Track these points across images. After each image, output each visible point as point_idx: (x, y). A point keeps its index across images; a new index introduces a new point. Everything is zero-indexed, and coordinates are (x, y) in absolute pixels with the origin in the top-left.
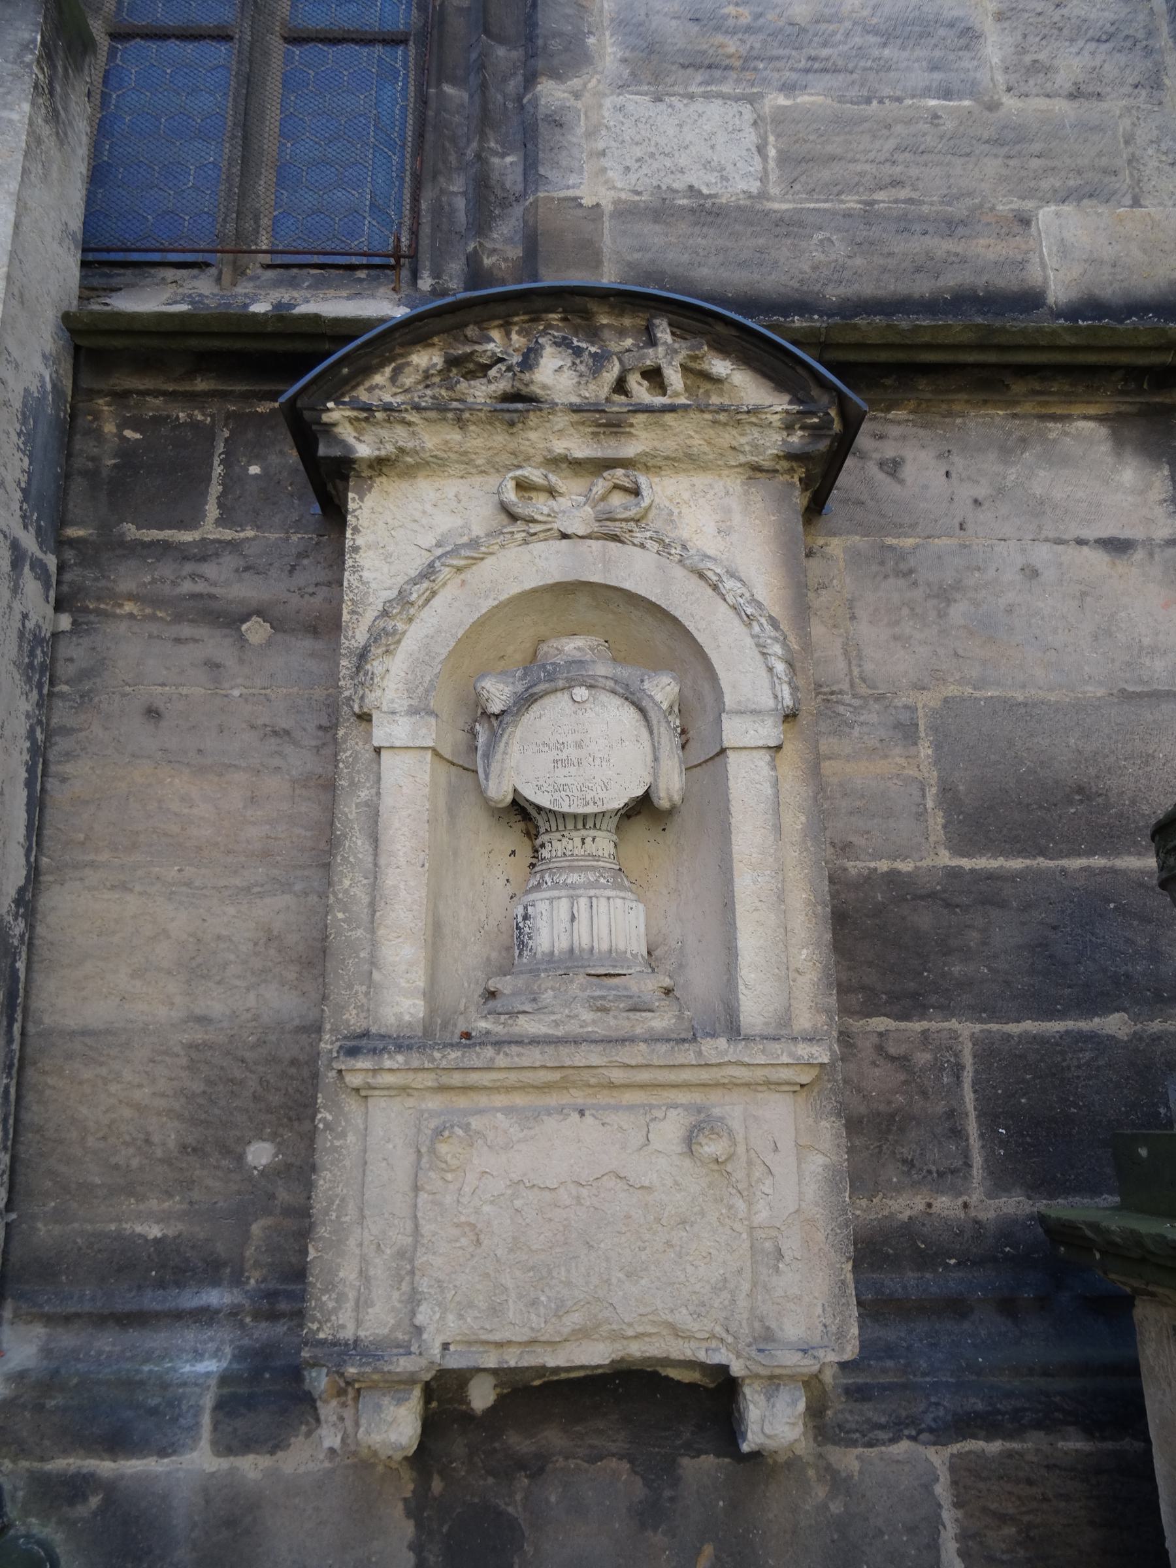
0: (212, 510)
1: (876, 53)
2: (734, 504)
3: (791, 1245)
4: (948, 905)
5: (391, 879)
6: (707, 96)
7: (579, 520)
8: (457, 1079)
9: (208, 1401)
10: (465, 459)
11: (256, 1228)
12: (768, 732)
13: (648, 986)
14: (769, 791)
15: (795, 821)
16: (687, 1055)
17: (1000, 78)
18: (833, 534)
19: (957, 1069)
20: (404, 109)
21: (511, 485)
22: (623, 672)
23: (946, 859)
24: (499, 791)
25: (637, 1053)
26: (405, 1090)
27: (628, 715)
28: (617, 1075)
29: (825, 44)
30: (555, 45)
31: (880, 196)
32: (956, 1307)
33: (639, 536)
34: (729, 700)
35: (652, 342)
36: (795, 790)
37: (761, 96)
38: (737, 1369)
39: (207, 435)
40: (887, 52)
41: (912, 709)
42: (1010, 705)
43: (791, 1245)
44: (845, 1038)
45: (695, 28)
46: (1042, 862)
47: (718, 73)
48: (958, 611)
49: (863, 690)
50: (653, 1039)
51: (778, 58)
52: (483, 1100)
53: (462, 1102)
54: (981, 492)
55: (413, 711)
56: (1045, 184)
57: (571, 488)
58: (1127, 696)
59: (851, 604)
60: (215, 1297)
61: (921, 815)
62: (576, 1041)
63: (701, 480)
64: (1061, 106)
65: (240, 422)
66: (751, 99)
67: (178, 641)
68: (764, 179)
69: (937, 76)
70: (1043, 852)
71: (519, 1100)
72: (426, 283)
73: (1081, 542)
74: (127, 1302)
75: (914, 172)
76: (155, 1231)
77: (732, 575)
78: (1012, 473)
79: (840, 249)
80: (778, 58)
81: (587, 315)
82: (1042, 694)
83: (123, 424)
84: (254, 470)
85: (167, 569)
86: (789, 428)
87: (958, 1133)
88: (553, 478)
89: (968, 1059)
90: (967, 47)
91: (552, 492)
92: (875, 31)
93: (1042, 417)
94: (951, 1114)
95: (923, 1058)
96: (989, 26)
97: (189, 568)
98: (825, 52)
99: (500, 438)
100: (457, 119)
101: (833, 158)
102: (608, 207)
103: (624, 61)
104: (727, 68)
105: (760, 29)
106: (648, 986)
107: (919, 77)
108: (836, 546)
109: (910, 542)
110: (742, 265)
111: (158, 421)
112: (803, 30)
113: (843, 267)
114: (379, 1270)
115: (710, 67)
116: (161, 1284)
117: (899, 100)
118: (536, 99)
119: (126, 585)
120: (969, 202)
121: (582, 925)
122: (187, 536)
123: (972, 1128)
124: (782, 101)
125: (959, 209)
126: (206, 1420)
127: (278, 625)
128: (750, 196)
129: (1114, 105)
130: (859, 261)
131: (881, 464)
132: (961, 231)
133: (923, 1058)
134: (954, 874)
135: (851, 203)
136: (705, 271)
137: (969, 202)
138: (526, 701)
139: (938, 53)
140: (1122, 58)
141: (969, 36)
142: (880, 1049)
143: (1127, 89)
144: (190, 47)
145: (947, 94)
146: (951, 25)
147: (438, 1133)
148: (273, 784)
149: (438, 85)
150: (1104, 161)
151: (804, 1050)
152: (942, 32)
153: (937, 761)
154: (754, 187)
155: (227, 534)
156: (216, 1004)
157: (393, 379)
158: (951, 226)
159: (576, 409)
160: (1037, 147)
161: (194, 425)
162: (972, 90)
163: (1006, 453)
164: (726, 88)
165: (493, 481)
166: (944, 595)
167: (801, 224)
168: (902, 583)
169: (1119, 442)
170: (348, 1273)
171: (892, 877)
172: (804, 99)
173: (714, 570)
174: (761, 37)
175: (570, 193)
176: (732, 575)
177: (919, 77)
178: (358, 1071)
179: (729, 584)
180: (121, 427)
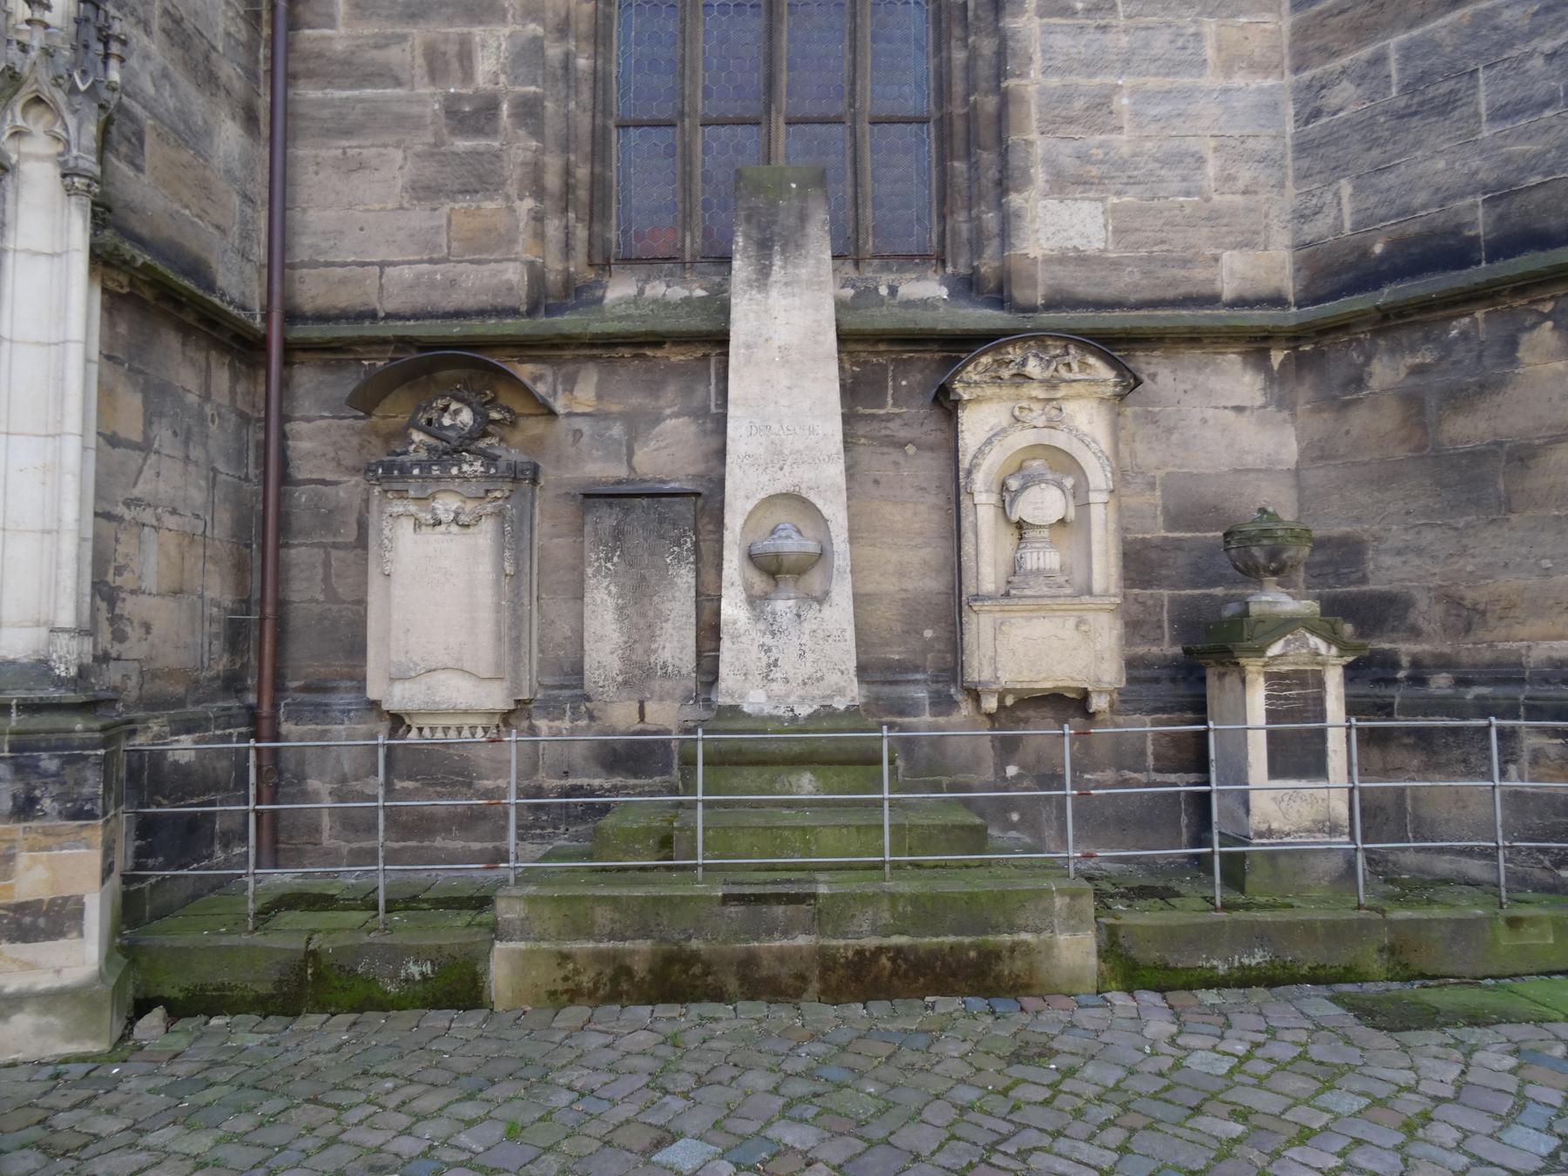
0: (890, 401)
1: (1158, 172)
2: (1094, 411)
3: (1107, 656)
4: (1163, 550)
5: (982, 547)
6: (1083, 199)
7: (1041, 422)
8: (1006, 608)
9: (927, 702)
10: (1000, 397)
11: (929, 656)
12: (1104, 497)
13: (1061, 580)
14: (1103, 516)
15: (1112, 526)
16: (1076, 601)
17: (1213, 184)
18: (1127, 406)
19: (1162, 607)
20: (930, 162)
21: (1017, 409)
22: (1057, 476)
23: (1163, 533)
24: (1015, 518)
25: (1062, 600)
26: (990, 611)
27: (1059, 492)
28: (1055, 607)
29: (1135, 169)
30: (1017, 174)
31: (1155, 249)
32: (1156, 680)
33: (1062, 427)
34: (1092, 486)
35: (1068, 354)
36: (1112, 516)
37: (1106, 198)
38: (1090, 689)
39: (884, 368)
40: (1163, 172)
41: (1154, 477)
42: (1191, 475)
43: (1107, 656)
44: (1125, 596)
45: (1078, 162)
46: (1198, 534)
47: (1088, 187)
48: (1175, 437)
49: (1136, 470)
50: (1066, 596)
51: (1113, 178)
52: (1013, 614)
53: (1007, 615)
54: (1188, 386)
55: (987, 491)
56: (1227, 240)
57: (1036, 407)
58: (1236, 471)
59: (1133, 435)
60: (918, 676)
61: (1155, 517)
62: (1042, 597)
63: (1082, 402)
64: (1238, 199)
65: (897, 362)
66: (1102, 200)
67: (883, 454)
68: (1106, 242)
69: (1185, 184)
70: (1198, 531)
71: (1024, 614)
72: (949, 270)
73: (1225, 408)
74: (890, 677)
75: (1171, 235)
76: (897, 657)
77: (1094, 442)
78: (1201, 379)
79: (1137, 276)
80: (1113, 178)
81: (1043, 341)
82: (1203, 471)
83: (853, 364)
84: (904, 383)
85: (875, 425)
86: (1116, 386)
87: (1160, 627)
88: (1032, 406)
89: (1166, 603)
90: (1199, 168)
91: (1030, 410)
92: (1157, 160)
93: (1215, 353)
94: (1159, 621)
95: (1150, 602)
97: (884, 424)
98: (1136, 173)
99: (1013, 391)
100: (960, 180)
101: (1136, 230)
102: (1040, 258)
103: (1047, 181)
104: (1092, 184)
105: (1107, 162)
106: (1061, 580)
107: (1176, 185)
108: (1129, 411)
109: (1157, 409)
110: (1096, 285)
111: (866, 362)
112: (1126, 161)
113: (1137, 285)
114: (985, 662)
115: (1085, 183)
116: (901, 673)
117: (1167, 198)
118: (1008, 203)
119: (861, 432)
120: (1193, 250)
121: (1041, 561)
122: (882, 412)
123: (1166, 625)
124: (1116, 201)
125: (1188, 254)
126: (927, 707)
127: (919, 447)
128: (1100, 250)
129: (1262, 197)
130: (1145, 282)
131: (1149, 376)
132: (1189, 265)
133: (1150, 602)
134: (1166, 538)
135: (1143, 253)
136: (1080, 288)
137: (1193, 250)
138: (1024, 488)
139: (1186, 172)
140: (1268, 171)
141: (1201, 160)
142: (1136, 600)
143: (1269, 188)
144: (824, 128)
145: (1188, 194)
146: (1193, 156)
147: (1002, 624)
148: (922, 508)
149: (951, 160)
150: (1254, 227)
151: (1112, 599)
152: (1189, 160)
153: (1162, 497)
154: (1102, 246)
155: (896, 410)
156: (909, 585)
157: (975, 368)
158: (1185, 263)
159: (1041, 382)
160: (1225, 221)
161: (880, 364)
162: (1199, 192)
163: (1199, 369)
164: (1091, 195)
165: (1010, 404)
166: (1169, 431)
167: (1121, 264)
168: (1153, 426)
169: (1245, 362)
170: (975, 663)
171: (1143, 540)
172: (1125, 199)
173: (1087, 440)
174: (1107, 166)
175: (1024, 251)
176: (1094, 442)
177: (1176, 185)
178: (977, 606)
179: (1093, 445)
180: (852, 365)
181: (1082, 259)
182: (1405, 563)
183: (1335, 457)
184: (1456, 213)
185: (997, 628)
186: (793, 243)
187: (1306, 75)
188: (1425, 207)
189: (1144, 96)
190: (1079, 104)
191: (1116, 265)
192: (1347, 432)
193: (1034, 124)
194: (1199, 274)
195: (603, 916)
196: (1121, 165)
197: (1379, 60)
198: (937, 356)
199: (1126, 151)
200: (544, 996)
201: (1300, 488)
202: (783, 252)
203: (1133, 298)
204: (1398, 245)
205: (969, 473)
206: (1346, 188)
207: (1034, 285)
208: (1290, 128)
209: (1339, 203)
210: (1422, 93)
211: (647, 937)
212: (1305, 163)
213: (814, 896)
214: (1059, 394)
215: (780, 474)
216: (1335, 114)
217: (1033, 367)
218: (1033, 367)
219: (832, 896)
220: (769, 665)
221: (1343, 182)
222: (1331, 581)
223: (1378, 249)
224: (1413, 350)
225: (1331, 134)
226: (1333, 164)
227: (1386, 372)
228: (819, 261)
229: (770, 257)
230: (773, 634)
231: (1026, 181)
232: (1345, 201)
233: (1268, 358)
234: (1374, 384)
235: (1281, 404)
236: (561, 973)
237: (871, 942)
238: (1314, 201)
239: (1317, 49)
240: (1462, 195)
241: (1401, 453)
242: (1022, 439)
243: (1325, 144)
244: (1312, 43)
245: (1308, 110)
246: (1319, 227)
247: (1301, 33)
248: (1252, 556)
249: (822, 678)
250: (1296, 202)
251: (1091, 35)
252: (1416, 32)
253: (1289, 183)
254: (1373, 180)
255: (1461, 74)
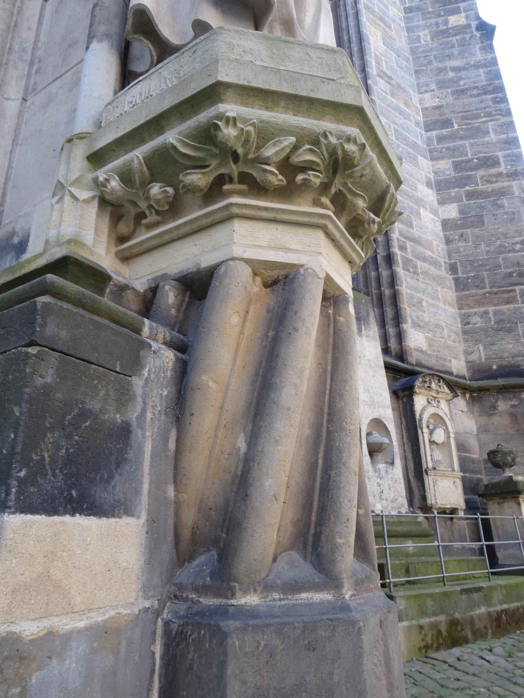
64: (452, 343)
66: (424, 333)
79: (435, 361)
96: (445, 327)
125: (445, 357)
135: (435, 354)
145: (442, 338)
158: (445, 360)
170: (429, 496)
177: (440, 335)
181: (422, 352)
182: (519, 468)
183: (490, 431)
184: (518, 361)
185: (435, 482)
186: (367, 323)
187: (463, 311)
188: (508, 357)
189: (429, 304)
190: (415, 301)
191: (429, 355)
192: (493, 424)
193: (406, 303)
194: (448, 364)
195: (430, 603)
196: (427, 323)
197: (486, 313)
198: (392, 375)
199: (427, 319)
200: (417, 650)
201: (479, 441)
202: (364, 325)
203: (435, 368)
204: (500, 367)
205: (421, 420)
206: (481, 348)
207: (412, 357)
208: (460, 325)
209: (479, 351)
210: (502, 325)
211: (443, 613)
212: (466, 337)
213: (482, 588)
214: (439, 396)
215: (374, 410)
216: (474, 324)
217: (433, 385)
218: (433, 385)
219: (487, 587)
220: (381, 492)
221: (480, 345)
222: (494, 474)
223: (495, 367)
224: (511, 400)
225: (474, 330)
226: (476, 339)
227: (503, 405)
228: (374, 330)
229: (360, 324)
230: (380, 478)
231: (406, 322)
232: (481, 351)
233: (465, 396)
234: (500, 408)
235: (471, 411)
236: (421, 637)
237: (499, 608)
238: (471, 349)
239: (466, 304)
240: (519, 357)
241: (512, 432)
242: (431, 410)
243: (473, 333)
244: (463, 302)
245: (465, 322)
246: (474, 357)
247: (459, 299)
248: (507, 460)
249: (396, 500)
250: (465, 348)
251: (415, 281)
252: (497, 308)
253: (462, 342)
254: (490, 347)
255: (513, 323)
